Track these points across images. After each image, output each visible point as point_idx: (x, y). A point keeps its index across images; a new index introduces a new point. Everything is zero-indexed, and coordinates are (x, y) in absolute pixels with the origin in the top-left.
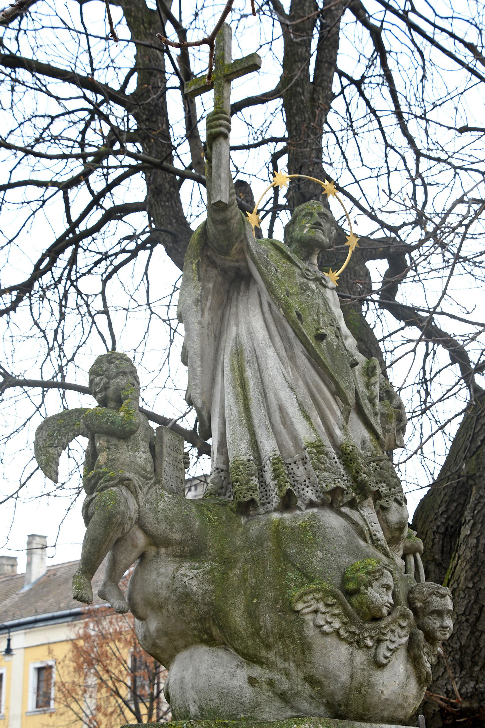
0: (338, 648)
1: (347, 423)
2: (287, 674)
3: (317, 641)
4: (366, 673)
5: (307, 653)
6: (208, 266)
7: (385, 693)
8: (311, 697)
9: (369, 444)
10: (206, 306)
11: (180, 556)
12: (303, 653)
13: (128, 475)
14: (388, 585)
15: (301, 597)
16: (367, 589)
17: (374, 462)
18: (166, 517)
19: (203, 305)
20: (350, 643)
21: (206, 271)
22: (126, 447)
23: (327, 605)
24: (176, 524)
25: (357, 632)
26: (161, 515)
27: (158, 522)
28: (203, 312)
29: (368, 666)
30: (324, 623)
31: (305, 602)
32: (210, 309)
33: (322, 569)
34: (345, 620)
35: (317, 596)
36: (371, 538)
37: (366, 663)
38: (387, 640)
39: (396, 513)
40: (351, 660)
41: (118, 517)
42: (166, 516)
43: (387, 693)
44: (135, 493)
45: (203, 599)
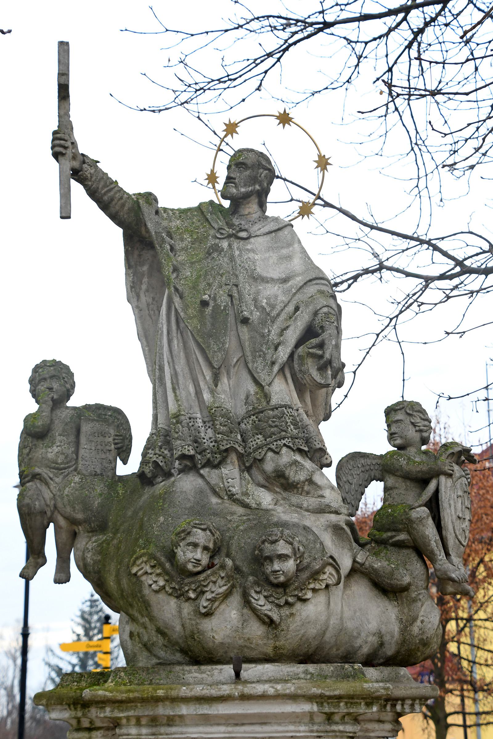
0: (168, 603)
1: (216, 386)
2: (145, 628)
3: (153, 599)
4: (194, 622)
5: (149, 609)
6: (143, 249)
7: (216, 637)
8: (165, 645)
9: (253, 398)
10: (141, 289)
11: (92, 532)
12: (147, 610)
13: (37, 470)
14: (193, 543)
15: (134, 563)
16: (177, 548)
17: (253, 415)
18: (69, 501)
19: (138, 290)
20: (177, 597)
21: (140, 256)
22: (42, 446)
23: (153, 567)
24: (76, 506)
25: (177, 587)
26: (66, 499)
27: (65, 506)
28: (138, 296)
29: (195, 616)
30: (152, 582)
31: (138, 566)
32: (147, 291)
33: (159, 533)
34: (167, 578)
35: (145, 559)
36: (227, 494)
37: (192, 613)
38: (207, 591)
39: (271, 463)
40: (180, 612)
41: (24, 509)
42: (69, 500)
43: (219, 638)
44: (47, 484)
45: (94, 569)
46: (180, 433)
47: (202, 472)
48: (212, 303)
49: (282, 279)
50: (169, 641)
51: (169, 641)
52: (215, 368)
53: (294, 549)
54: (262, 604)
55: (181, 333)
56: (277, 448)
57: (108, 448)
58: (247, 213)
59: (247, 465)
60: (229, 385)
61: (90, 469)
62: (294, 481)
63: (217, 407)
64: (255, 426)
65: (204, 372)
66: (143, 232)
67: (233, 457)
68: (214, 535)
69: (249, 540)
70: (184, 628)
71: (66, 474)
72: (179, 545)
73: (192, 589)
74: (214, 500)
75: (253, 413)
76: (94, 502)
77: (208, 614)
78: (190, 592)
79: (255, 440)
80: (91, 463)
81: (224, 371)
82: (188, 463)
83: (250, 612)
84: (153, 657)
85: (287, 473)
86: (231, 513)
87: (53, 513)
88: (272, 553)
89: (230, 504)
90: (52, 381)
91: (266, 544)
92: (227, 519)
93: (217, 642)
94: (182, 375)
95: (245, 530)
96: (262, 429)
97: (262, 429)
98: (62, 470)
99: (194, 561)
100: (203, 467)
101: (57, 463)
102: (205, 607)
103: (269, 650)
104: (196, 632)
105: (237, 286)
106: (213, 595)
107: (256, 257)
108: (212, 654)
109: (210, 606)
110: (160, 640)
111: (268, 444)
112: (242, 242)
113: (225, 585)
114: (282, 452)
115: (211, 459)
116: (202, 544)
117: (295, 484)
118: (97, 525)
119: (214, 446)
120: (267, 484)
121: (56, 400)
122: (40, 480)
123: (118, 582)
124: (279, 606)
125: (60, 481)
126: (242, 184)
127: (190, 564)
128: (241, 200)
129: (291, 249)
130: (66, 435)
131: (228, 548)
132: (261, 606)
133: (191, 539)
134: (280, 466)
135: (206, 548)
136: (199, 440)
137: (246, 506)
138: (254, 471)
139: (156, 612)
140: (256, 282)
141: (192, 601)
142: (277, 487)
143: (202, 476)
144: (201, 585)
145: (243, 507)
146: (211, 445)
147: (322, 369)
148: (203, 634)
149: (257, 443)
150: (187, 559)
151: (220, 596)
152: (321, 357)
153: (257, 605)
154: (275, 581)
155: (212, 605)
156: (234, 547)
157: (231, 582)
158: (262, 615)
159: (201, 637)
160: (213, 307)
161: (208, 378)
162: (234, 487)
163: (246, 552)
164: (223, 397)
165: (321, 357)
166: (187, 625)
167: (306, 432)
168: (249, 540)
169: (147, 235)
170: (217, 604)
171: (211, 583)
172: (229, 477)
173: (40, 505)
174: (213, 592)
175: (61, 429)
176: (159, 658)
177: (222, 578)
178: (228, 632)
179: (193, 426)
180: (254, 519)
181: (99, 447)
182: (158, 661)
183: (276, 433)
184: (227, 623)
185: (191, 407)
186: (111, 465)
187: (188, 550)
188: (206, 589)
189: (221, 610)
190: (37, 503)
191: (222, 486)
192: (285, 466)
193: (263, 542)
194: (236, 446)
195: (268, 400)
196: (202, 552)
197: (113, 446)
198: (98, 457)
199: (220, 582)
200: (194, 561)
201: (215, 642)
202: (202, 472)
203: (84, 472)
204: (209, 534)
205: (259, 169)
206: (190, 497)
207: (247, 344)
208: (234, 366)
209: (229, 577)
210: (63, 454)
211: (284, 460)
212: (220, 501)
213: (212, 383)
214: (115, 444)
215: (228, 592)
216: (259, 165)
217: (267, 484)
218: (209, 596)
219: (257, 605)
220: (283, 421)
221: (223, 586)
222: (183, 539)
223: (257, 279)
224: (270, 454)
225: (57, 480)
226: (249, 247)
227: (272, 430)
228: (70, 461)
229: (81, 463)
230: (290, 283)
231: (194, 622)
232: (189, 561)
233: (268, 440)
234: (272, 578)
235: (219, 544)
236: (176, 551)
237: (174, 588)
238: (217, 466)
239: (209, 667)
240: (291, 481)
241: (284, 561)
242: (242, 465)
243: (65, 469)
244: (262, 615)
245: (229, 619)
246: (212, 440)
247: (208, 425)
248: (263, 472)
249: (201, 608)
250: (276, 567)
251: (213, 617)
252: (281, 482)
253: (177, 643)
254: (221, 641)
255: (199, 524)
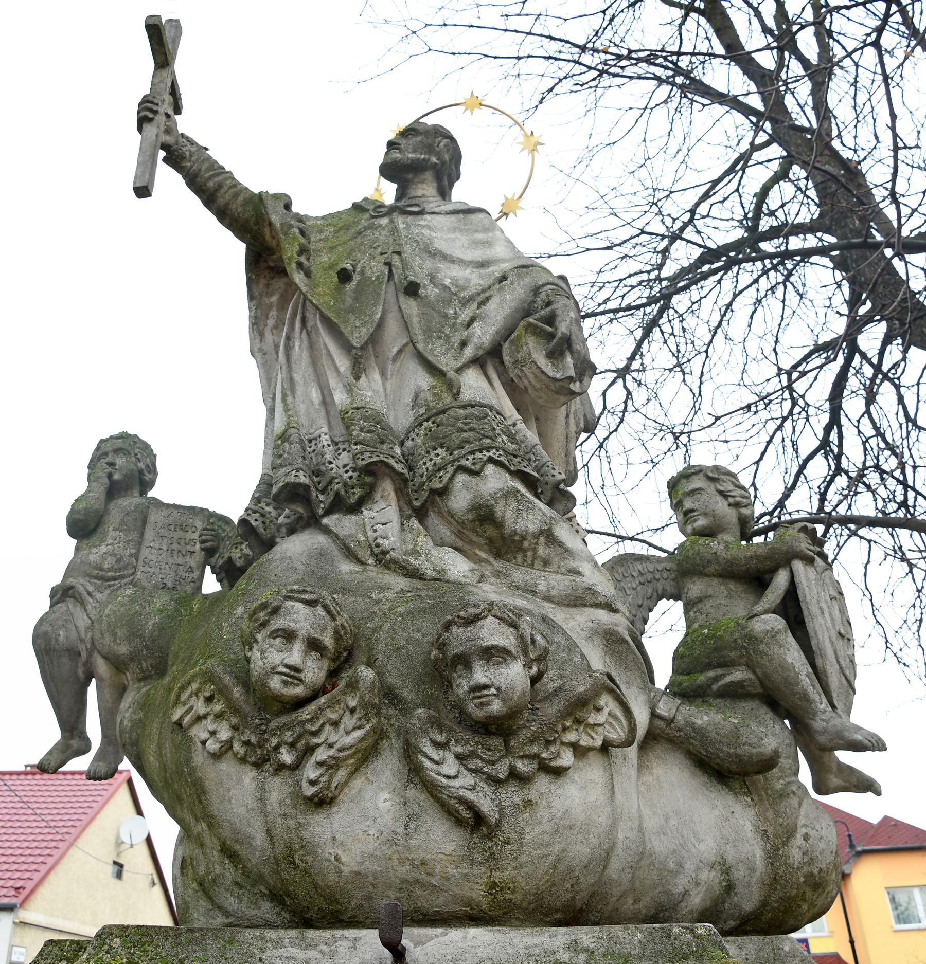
1: (357, 378)
4: (291, 823)
6: (272, 278)
7: (344, 859)
8: (237, 883)
12: (200, 801)
14: (284, 630)
17: (427, 420)
29: (295, 807)
36: (373, 554)
37: (288, 801)
38: (318, 745)
39: (464, 492)
40: (262, 800)
43: (350, 860)
46: (286, 455)
47: (325, 521)
48: (356, 278)
49: (477, 262)
50: (246, 873)
51: (246, 873)
52: (355, 348)
53: (522, 638)
54: (452, 772)
55: (308, 334)
56: (474, 464)
57: (189, 548)
58: (420, 194)
59: (417, 504)
60: (385, 390)
61: (156, 579)
62: (515, 531)
63: (358, 408)
64: (431, 436)
65: (337, 362)
66: (268, 237)
67: (387, 488)
68: (333, 618)
69: (419, 636)
70: (271, 838)
71: (115, 587)
72: (256, 641)
73: (286, 744)
74: (346, 567)
75: (425, 416)
76: (147, 622)
77: (322, 802)
78: (283, 750)
79: (431, 460)
80: (158, 570)
81: (374, 364)
82: (301, 510)
83: (423, 796)
84: (217, 912)
85: (499, 510)
86: (379, 587)
87: (90, 655)
88: (468, 645)
89: (378, 573)
90: (123, 468)
91: (454, 629)
92: (370, 598)
93: (346, 870)
94: (302, 383)
95: (409, 613)
96: (444, 437)
97: (444, 437)
98: (108, 580)
99: (285, 670)
100: (328, 512)
101: (102, 569)
102: (313, 783)
103: (477, 893)
104: (297, 847)
105: (399, 253)
106: (332, 752)
107: (433, 234)
108: (337, 901)
109: (324, 779)
110: (228, 873)
111: (458, 460)
112: (410, 219)
113: (359, 727)
114: (487, 473)
115: (342, 492)
116: (302, 633)
117: (517, 538)
118: (151, 666)
119: (351, 478)
120: (460, 544)
121: (117, 482)
122: (75, 598)
123: (160, 755)
124: (495, 781)
125: (104, 599)
126: (411, 150)
127: (276, 677)
128: (410, 176)
129: (490, 234)
130: (125, 530)
131: (371, 648)
132: (448, 777)
133: (279, 623)
134: (482, 496)
135: (314, 645)
136: (323, 468)
137: (414, 574)
138: (433, 519)
139: (216, 807)
140: (434, 259)
141: (286, 773)
142: (480, 550)
143: (327, 531)
144: (306, 731)
145: (405, 576)
146: (346, 476)
147: (555, 355)
148: (313, 853)
149: (435, 464)
150: (268, 667)
151: (345, 753)
152: (552, 336)
153: (439, 774)
154: (479, 714)
155: (331, 776)
156: (381, 646)
157: (374, 720)
158: (452, 801)
159: (309, 858)
160: (359, 281)
161: (342, 369)
162: (386, 538)
163: (410, 657)
164: (369, 394)
165: (552, 336)
166: (278, 831)
167: (533, 458)
168: (419, 636)
169: (274, 243)
170: (341, 774)
171: (327, 727)
172: (378, 521)
173: (67, 638)
174: (331, 746)
175: (118, 521)
176: (227, 914)
177: (353, 711)
178: (372, 845)
179: (314, 451)
180: (430, 597)
181: (175, 546)
182: (227, 921)
183: (471, 439)
184: (369, 824)
185: (312, 422)
186: (192, 575)
187: (271, 646)
188: (316, 740)
189: (354, 791)
190: (61, 632)
191: (363, 539)
192: (493, 496)
193: (447, 627)
194: (392, 462)
195: (455, 391)
196: (306, 654)
197: (198, 546)
198: (171, 561)
199: (349, 721)
200: (285, 670)
201: (341, 871)
202: (325, 521)
203: (145, 583)
204: (324, 614)
205: (436, 137)
206: (297, 564)
207: (415, 320)
208: (394, 360)
209: (368, 709)
210: (113, 555)
211: (490, 486)
212: (358, 568)
213: (348, 374)
214: (202, 542)
215: (365, 744)
216: (436, 133)
217: (460, 544)
218: (321, 754)
219: (439, 774)
220: (486, 424)
221: (354, 729)
222: (264, 625)
223: (435, 254)
224: (461, 478)
225: (98, 596)
226: (422, 223)
227: (464, 435)
228: (125, 568)
229: (142, 569)
230: (490, 269)
231: (291, 823)
232: (273, 671)
233: (456, 452)
234: (471, 707)
235: (348, 640)
236: (249, 654)
237: (247, 743)
238: (355, 509)
239: (327, 934)
240: (507, 531)
241: (499, 663)
242: (405, 508)
243: (115, 579)
244: (452, 801)
245: (372, 813)
246: (348, 468)
247: (341, 446)
248: (450, 516)
249: (305, 784)
250: (480, 675)
251: (335, 809)
252: (488, 534)
253: (260, 878)
254: (356, 869)
255: (298, 591)
